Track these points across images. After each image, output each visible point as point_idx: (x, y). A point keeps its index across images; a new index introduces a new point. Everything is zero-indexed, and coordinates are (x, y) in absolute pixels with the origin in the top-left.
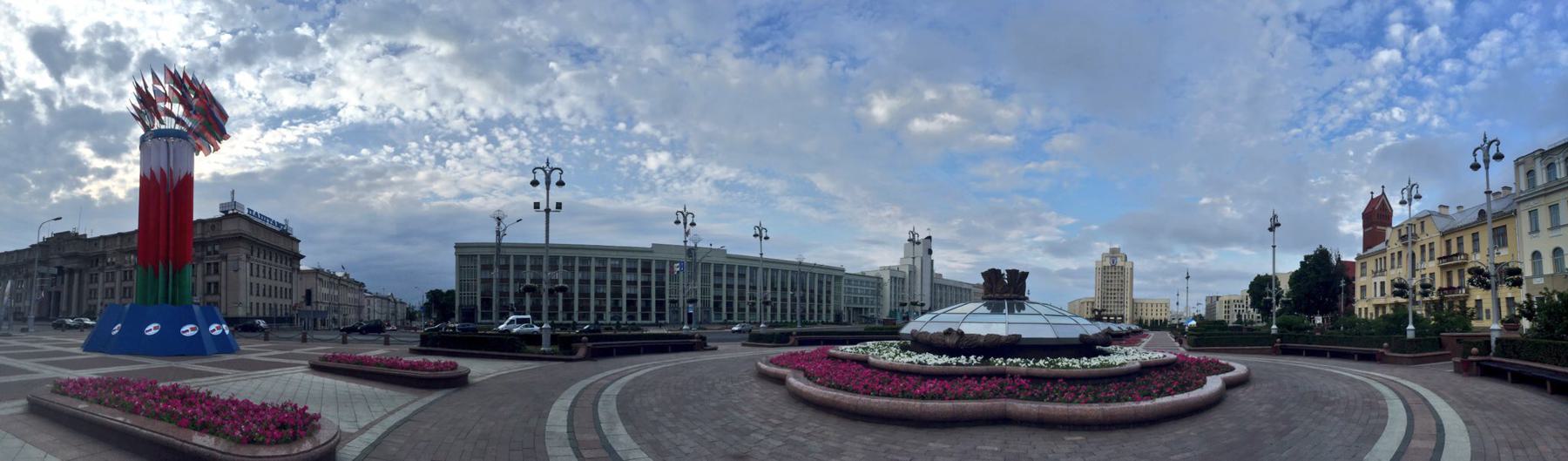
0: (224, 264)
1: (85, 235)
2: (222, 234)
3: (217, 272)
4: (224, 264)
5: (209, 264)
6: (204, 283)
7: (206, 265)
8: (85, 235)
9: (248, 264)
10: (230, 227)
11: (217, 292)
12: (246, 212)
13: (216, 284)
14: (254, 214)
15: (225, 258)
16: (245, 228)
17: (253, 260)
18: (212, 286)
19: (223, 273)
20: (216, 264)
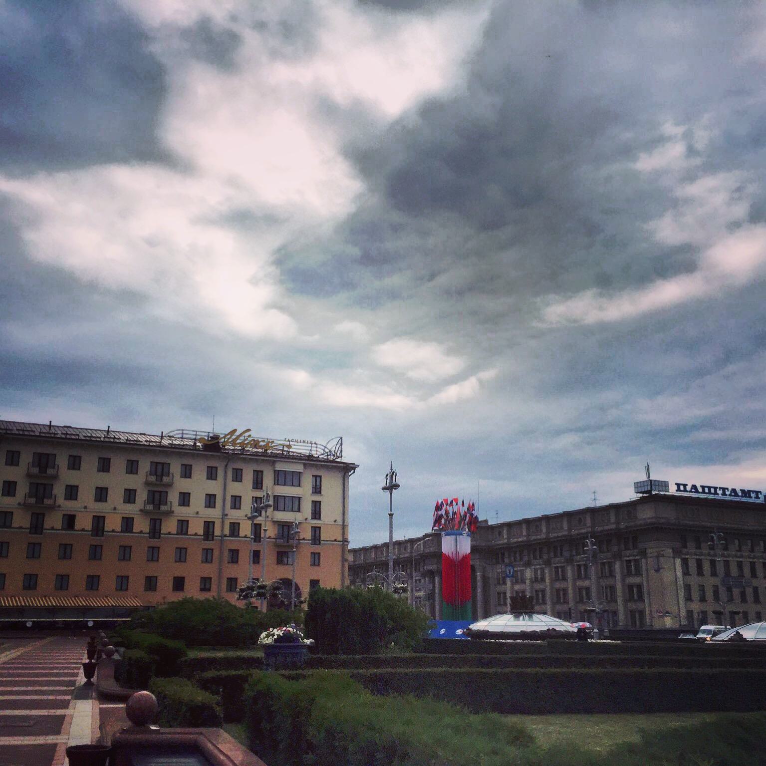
0: (643, 560)
1: (486, 521)
2: (639, 523)
3: (638, 573)
4: (643, 560)
5: (629, 561)
6: (623, 585)
7: (625, 564)
8: (486, 521)
9: (678, 562)
10: (646, 514)
11: (641, 598)
12: (672, 490)
13: (640, 587)
14: (700, 490)
15: (644, 553)
16: (669, 514)
17: (688, 554)
18: (635, 590)
19: (644, 573)
20: (636, 561)
